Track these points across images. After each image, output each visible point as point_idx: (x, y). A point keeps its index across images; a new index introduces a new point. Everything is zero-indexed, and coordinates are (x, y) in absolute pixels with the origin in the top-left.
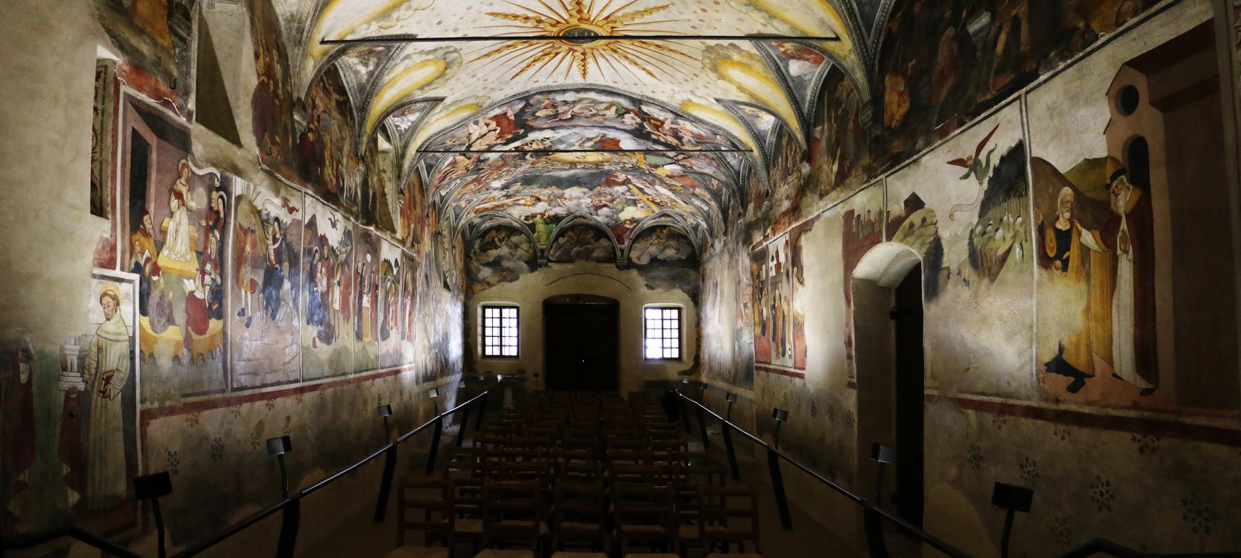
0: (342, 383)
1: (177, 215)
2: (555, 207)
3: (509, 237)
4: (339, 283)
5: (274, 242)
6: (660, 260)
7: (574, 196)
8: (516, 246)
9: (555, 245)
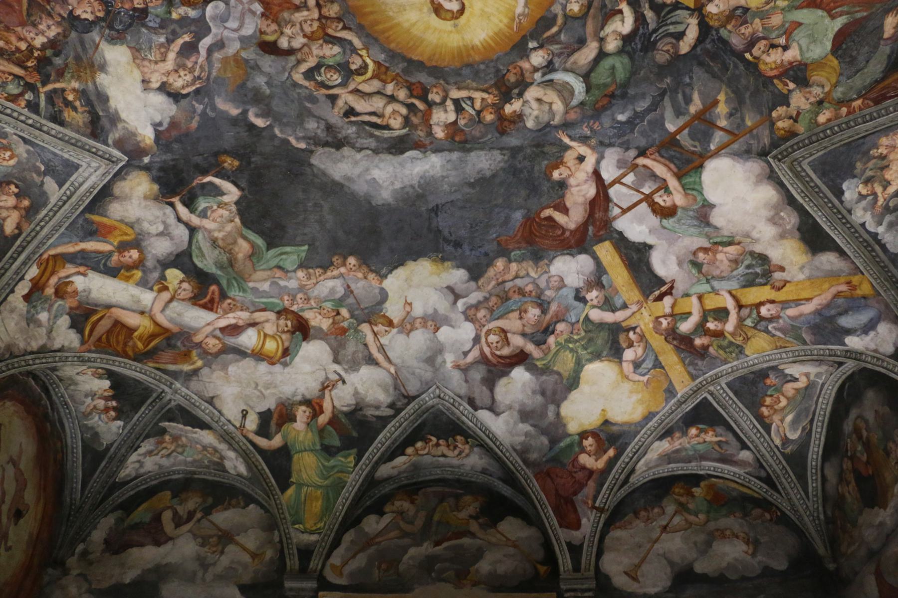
2: (354, 366)
3: (207, 511)
6: (704, 578)
7: (418, 310)
8: (226, 538)
9: (348, 537)
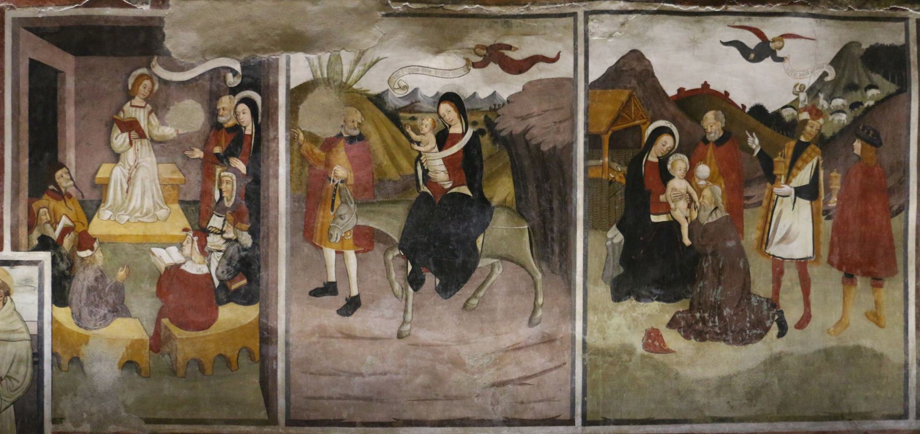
1: (130, 156)
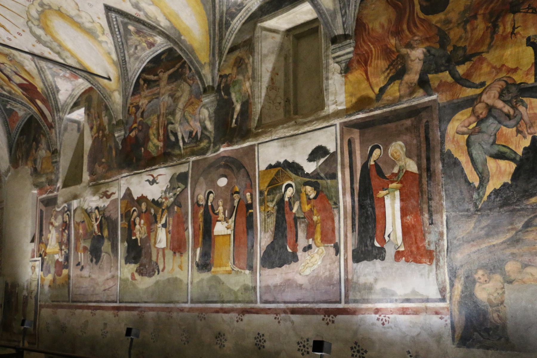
0: (170, 310)
4: (164, 226)
5: (96, 221)
